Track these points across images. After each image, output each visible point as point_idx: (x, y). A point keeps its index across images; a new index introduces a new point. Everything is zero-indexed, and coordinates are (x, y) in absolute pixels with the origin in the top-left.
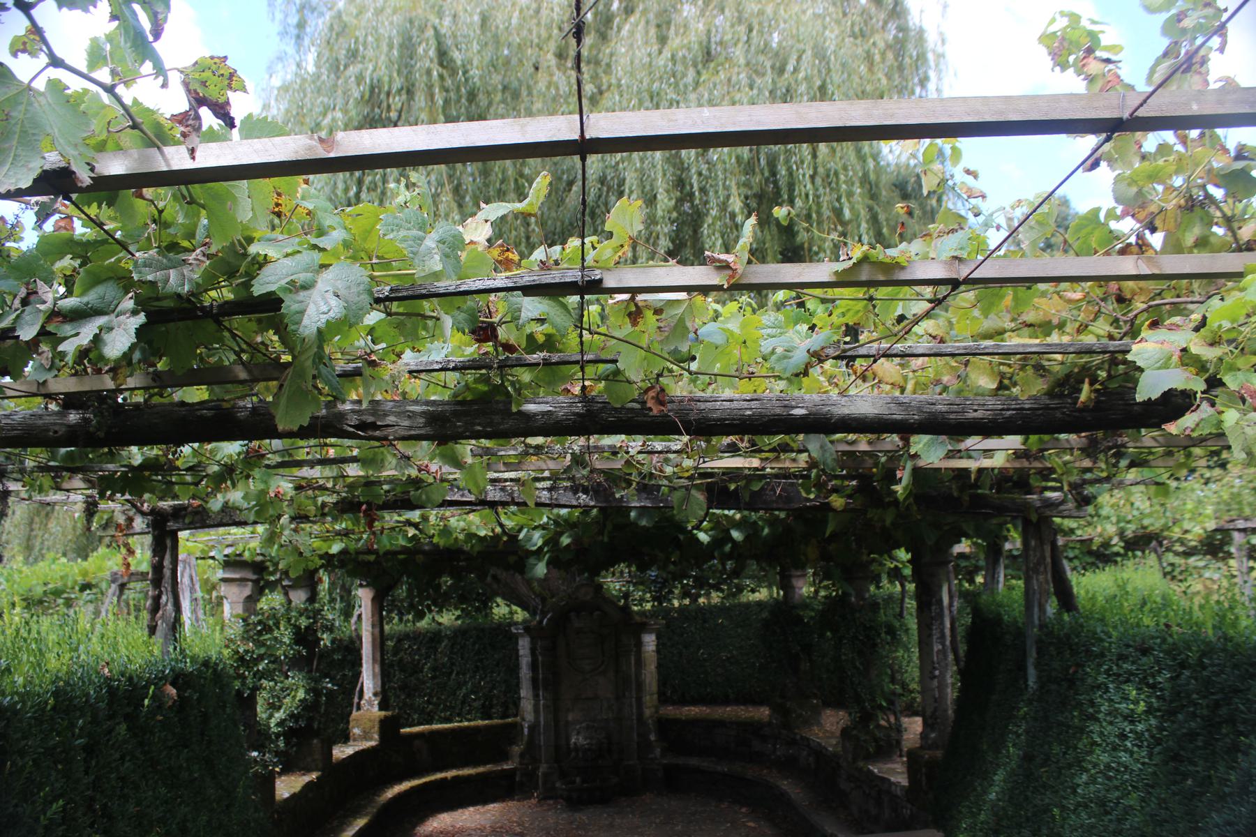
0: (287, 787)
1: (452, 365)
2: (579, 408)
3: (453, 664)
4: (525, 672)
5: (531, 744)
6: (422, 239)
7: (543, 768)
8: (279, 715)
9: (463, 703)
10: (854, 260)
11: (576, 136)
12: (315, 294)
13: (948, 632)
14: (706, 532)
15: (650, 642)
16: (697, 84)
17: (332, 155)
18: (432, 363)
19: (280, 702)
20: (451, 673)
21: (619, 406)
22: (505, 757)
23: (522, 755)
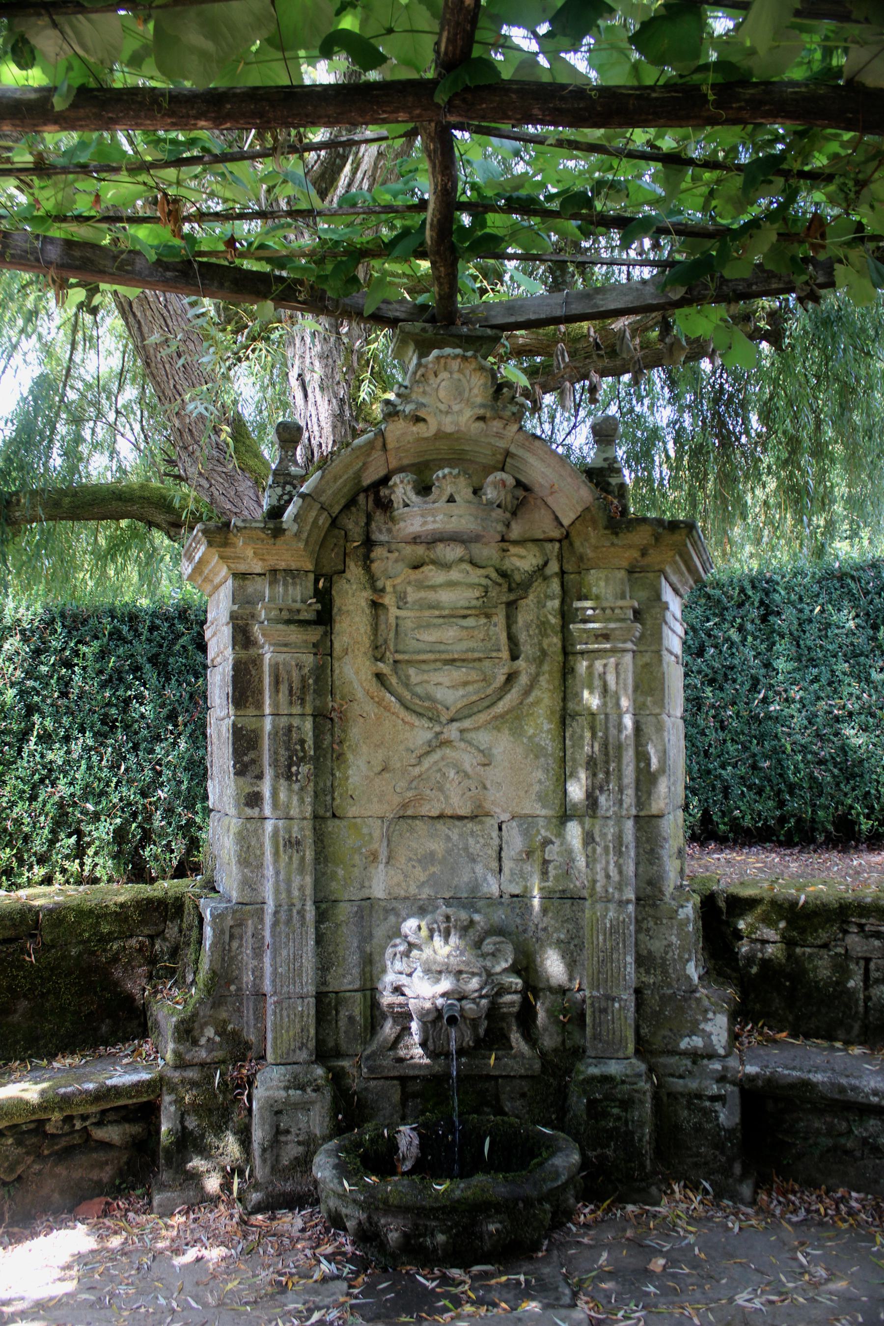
3: (31, 710)
5: (222, 983)
7: (268, 1085)
9: (61, 821)
20: (24, 736)
23: (186, 1032)
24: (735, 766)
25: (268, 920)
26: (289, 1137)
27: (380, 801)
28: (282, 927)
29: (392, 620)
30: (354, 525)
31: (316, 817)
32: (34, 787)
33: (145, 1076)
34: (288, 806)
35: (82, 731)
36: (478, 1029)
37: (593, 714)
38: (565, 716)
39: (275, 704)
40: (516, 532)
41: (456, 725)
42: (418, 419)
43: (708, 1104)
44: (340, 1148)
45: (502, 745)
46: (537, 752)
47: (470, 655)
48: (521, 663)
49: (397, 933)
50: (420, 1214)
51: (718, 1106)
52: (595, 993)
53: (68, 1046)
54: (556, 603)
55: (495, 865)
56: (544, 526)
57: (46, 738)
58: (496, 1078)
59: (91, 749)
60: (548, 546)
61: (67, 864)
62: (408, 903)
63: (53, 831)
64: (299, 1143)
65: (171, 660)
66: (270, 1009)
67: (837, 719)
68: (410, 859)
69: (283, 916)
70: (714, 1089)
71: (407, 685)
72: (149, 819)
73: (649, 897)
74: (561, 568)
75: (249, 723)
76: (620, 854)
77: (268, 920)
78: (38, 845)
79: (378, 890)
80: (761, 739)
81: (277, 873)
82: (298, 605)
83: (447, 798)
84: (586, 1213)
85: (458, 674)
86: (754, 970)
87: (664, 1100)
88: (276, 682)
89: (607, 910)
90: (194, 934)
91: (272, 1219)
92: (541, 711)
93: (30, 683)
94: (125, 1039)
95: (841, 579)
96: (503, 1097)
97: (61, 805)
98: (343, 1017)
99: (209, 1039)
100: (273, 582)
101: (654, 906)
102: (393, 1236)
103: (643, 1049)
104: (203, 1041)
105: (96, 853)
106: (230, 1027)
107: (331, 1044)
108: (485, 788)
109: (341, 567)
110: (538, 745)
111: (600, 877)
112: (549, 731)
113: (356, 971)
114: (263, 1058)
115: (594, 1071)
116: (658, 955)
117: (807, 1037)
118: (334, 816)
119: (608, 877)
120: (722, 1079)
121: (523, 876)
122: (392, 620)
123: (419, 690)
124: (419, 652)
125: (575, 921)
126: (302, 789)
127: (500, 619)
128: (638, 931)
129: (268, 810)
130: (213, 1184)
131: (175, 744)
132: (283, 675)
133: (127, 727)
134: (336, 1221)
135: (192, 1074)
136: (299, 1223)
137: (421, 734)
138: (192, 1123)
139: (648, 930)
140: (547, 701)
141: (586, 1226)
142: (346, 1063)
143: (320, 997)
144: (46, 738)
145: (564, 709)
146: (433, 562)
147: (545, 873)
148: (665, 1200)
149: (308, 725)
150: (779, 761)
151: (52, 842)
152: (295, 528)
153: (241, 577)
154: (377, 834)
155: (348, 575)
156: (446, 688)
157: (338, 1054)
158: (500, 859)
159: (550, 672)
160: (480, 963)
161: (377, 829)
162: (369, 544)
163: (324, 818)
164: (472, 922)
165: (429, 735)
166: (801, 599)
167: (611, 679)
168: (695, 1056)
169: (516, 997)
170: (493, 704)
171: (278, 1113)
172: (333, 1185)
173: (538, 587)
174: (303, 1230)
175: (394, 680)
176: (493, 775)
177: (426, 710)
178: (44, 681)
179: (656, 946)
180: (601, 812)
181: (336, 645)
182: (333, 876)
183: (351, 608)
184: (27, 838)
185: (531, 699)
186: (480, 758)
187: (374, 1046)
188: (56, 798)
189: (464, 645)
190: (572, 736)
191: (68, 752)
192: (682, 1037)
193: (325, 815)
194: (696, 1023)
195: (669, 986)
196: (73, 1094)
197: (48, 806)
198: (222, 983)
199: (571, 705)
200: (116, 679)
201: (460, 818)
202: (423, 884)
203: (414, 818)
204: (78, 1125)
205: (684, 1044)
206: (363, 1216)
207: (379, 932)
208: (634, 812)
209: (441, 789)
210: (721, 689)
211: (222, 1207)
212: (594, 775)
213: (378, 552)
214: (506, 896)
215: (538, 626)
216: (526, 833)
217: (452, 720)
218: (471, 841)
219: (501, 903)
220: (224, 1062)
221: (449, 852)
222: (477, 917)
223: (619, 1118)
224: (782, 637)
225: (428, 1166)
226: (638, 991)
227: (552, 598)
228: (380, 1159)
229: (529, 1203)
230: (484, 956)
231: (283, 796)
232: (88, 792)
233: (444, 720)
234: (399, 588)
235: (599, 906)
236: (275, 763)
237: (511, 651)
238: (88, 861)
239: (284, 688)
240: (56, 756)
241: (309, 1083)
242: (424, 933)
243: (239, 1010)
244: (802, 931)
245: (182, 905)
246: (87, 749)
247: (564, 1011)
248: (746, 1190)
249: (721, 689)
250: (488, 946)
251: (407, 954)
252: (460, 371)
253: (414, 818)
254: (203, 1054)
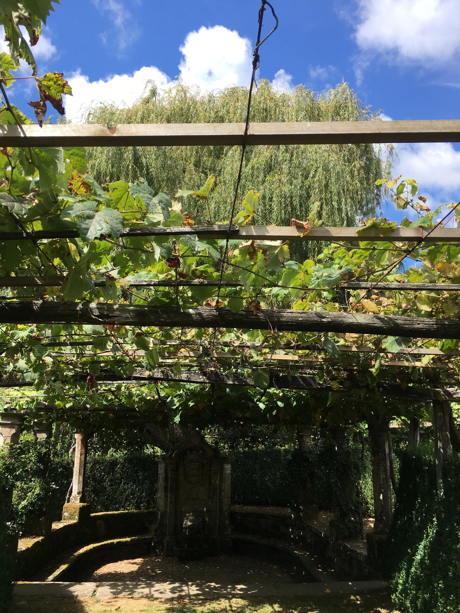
0: (24, 544)
1: (153, 283)
2: (215, 313)
4: (161, 483)
6: (151, 199)
7: (167, 538)
8: (24, 503)
9: (126, 500)
10: (367, 226)
11: (242, 133)
12: (94, 221)
13: (388, 468)
14: (264, 403)
15: (228, 468)
16: (264, 181)
17: (115, 135)
18: (142, 282)
19: (26, 495)
21: (234, 312)
22: (145, 531)
23: (156, 531)
25: (168, 514)
49: (186, 516)
77: (168, 514)
153: (166, 464)
178: (124, 472)
184: (121, 503)
240: (126, 487)
246: (131, 485)
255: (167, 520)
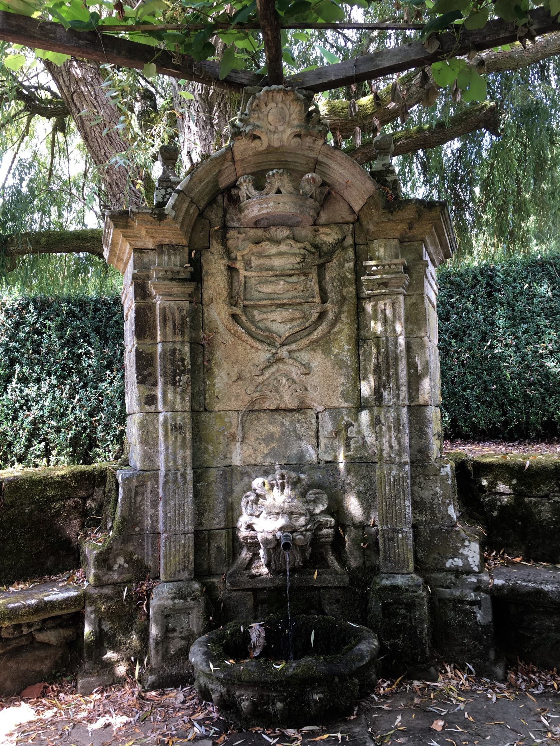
3: (13, 361)
7: (161, 596)
9: (34, 434)
22: (68, 558)
23: (104, 561)
24: (472, 389)
25: (161, 480)
26: (175, 634)
27: (236, 400)
28: (170, 484)
29: (242, 279)
30: (215, 216)
31: (193, 411)
32: (16, 411)
33: (73, 593)
34: (174, 403)
35: (49, 375)
36: (305, 552)
37: (378, 337)
38: (359, 340)
39: (164, 335)
40: (324, 217)
41: (286, 348)
42: (256, 137)
43: (468, 607)
44: (209, 640)
45: (317, 361)
46: (340, 364)
47: (294, 301)
48: (329, 305)
49: (249, 488)
50: (264, 686)
51: (475, 609)
52: (385, 528)
53: (21, 577)
54: (352, 264)
55: (314, 441)
56: (344, 214)
57: (24, 380)
58: (318, 588)
59: (55, 386)
60: (346, 227)
61: (38, 461)
62: (257, 469)
63: (29, 440)
64: (182, 638)
65: (108, 330)
66: (163, 542)
67: (542, 356)
68: (258, 439)
69: (171, 478)
70: (472, 596)
71: (253, 322)
72: (94, 431)
73: (420, 461)
74: (354, 241)
75: (148, 349)
76: (398, 431)
77: (161, 480)
78: (18, 449)
79: (237, 460)
80: (490, 370)
81: (167, 448)
82: (178, 268)
83: (281, 397)
84: (384, 687)
85: (287, 314)
86: (495, 514)
87: (437, 603)
88: (164, 320)
89: (391, 469)
90: (113, 495)
91: (162, 695)
92: (343, 337)
93: (12, 344)
94: (63, 570)
95: (542, 266)
96: (323, 602)
97: (34, 422)
98: (213, 547)
99: (120, 566)
100: (161, 253)
101: (423, 467)
102: (245, 704)
103: (420, 567)
104: (116, 567)
105: (59, 454)
106: (135, 557)
107: (206, 567)
108: (306, 389)
109: (207, 245)
110: (341, 360)
111: (386, 446)
112: (348, 350)
113: (221, 515)
114: (158, 578)
115: (386, 582)
116: (427, 501)
117: (536, 560)
118: (206, 410)
119: (391, 447)
120: (477, 588)
121: (335, 450)
122: (242, 279)
123: (261, 325)
124: (260, 300)
125: (370, 478)
126: (183, 391)
127: (314, 276)
128: (413, 484)
129: (160, 407)
130: (121, 670)
131: (111, 383)
132: (169, 315)
133: (79, 372)
134: (205, 695)
135: (107, 591)
136: (181, 697)
137: (263, 355)
138: (107, 626)
139: (420, 483)
140: (346, 331)
141: (385, 696)
142: (215, 580)
143: (197, 534)
144: (24, 380)
145: (358, 335)
146: (268, 240)
147: (348, 446)
148: (441, 678)
149: (187, 349)
150: (502, 385)
151: (28, 448)
152: (174, 213)
153: (139, 251)
154: (235, 422)
155: (212, 249)
156: (279, 323)
157: (211, 574)
158: (317, 437)
159: (348, 311)
160: (306, 507)
161: (235, 419)
162: (225, 228)
163: (199, 412)
164: (299, 480)
165: (268, 355)
166: (515, 281)
167: (389, 313)
168: (457, 572)
169: (330, 531)
170: (310, 333)
171: (167, 616)
172: (202, 667)
173: (339, 254)
174: (184, 702)
175: (244, 318)
176: (312, 380)
177: (267, 338)
178: (23, 343)
179: (426, 495)
180: (385, 403)
181: (205, 296)
182: (206, 451)
183: (214, 271)
184: (10, 445)
185: (336, 330)
186: (303, 370)
187: (235, 567)
188: (31, 418)
189: (291, 294)
190: (364, 353)
191: (39, 388)
192: (447, 559)
193: (200, 409)
194: (457, 549)
195: (437, 523)
196: (19, 607)
197: (25, 424)
198: (130, 527)
199: (362, 333)
200: (72, 342)
201: (291, 410)
202: (267, 454)
203: (259, 411)
204: (25, 631)
205: (448, 564)
206: (224, 690)
207: (237, 489)
208: (407, 402)
209: (277, 391)
210: (461, 340)
211: (127, 687)
212: (380, 378)
213: (232, 233)
214: (323, 462)
215: (339, 280)
216: (335, 419)
217: (283, 345)
218: (298, 426)
219: (319, 467)
220: (130, 581)
221: (283, 433)
222: (303, 476)
223: (405, 617)
224: (502, 305)
225: (271, 652)
226: (414, 526)
227: (349, 262)
228: (238, 648)
229: (343, 678)
230: (307, 502)
231: (170, 396)
232: (53, 414)
233: (278, 345)
234: (246, 257)
235: (385, 467)
236: (164, 374)
237: (321, 297)
238: (52, 459)
239: (169, 324)
240: (31, 391)
241: (189, 594)
242: (267, 487)
243: (141, 545)
244: (529, 486)
245: (105, 476)
246: (52, 387)
247: (364, 541)
248: (499, 671)
249: (461, 340)
250: (310, 496)
251: (256, 502)
252: (283, 101)
253: (259, 411)
254: (116, 576)
255: (160, 509)
